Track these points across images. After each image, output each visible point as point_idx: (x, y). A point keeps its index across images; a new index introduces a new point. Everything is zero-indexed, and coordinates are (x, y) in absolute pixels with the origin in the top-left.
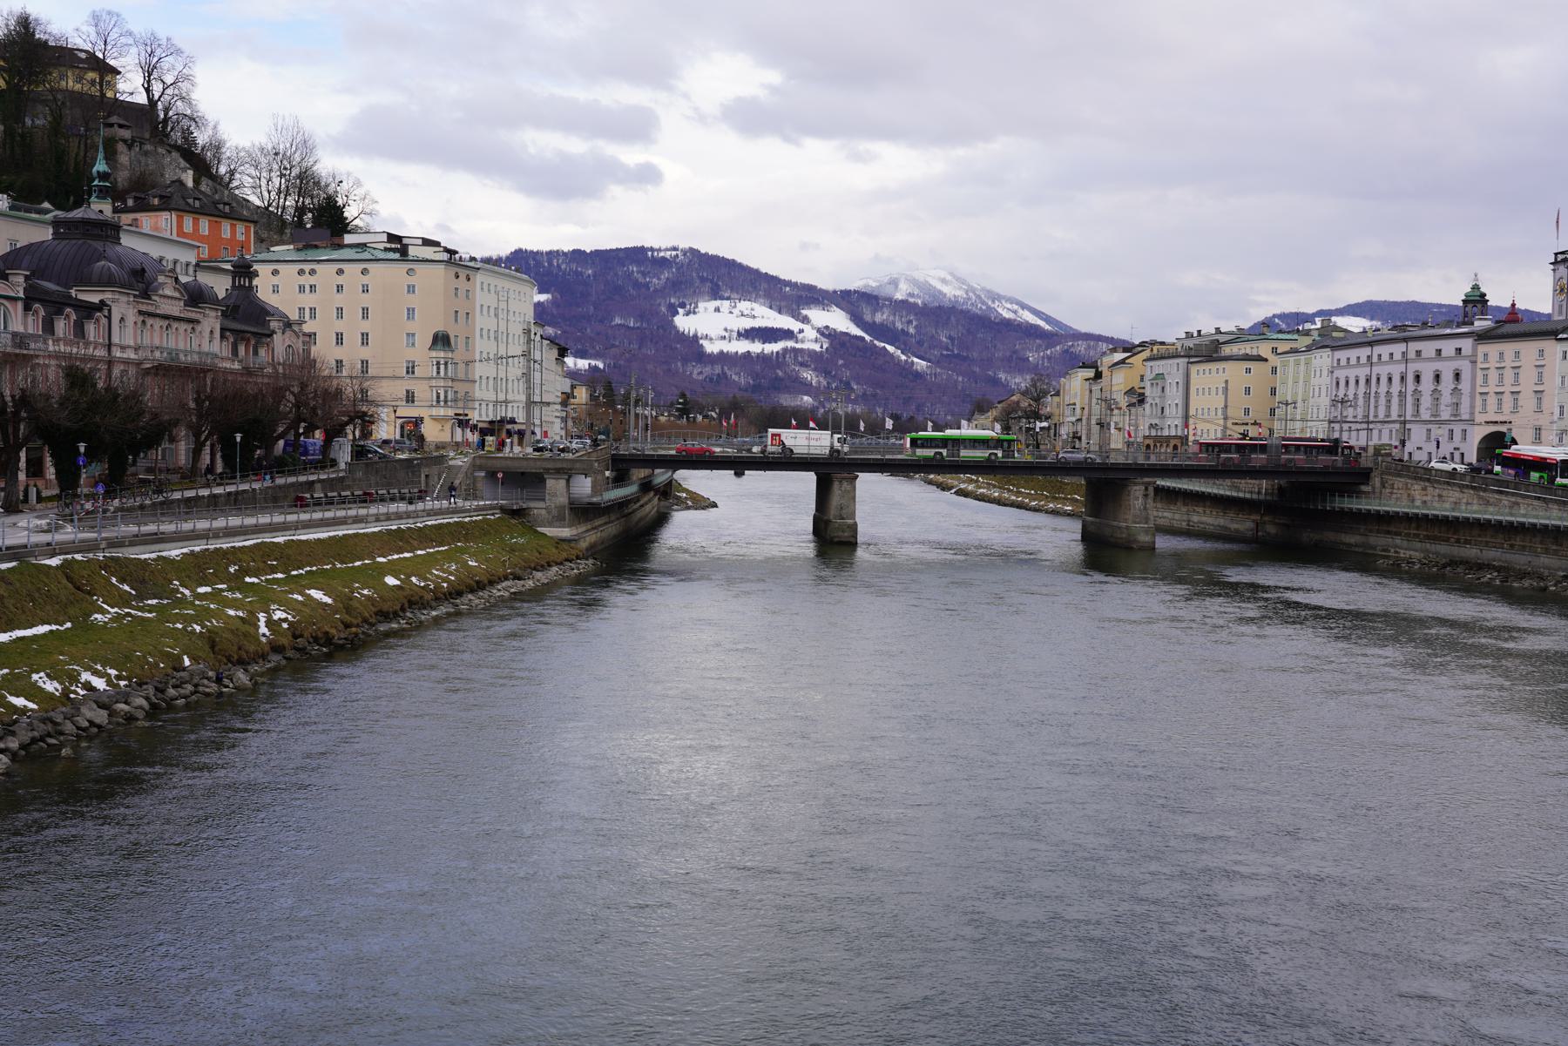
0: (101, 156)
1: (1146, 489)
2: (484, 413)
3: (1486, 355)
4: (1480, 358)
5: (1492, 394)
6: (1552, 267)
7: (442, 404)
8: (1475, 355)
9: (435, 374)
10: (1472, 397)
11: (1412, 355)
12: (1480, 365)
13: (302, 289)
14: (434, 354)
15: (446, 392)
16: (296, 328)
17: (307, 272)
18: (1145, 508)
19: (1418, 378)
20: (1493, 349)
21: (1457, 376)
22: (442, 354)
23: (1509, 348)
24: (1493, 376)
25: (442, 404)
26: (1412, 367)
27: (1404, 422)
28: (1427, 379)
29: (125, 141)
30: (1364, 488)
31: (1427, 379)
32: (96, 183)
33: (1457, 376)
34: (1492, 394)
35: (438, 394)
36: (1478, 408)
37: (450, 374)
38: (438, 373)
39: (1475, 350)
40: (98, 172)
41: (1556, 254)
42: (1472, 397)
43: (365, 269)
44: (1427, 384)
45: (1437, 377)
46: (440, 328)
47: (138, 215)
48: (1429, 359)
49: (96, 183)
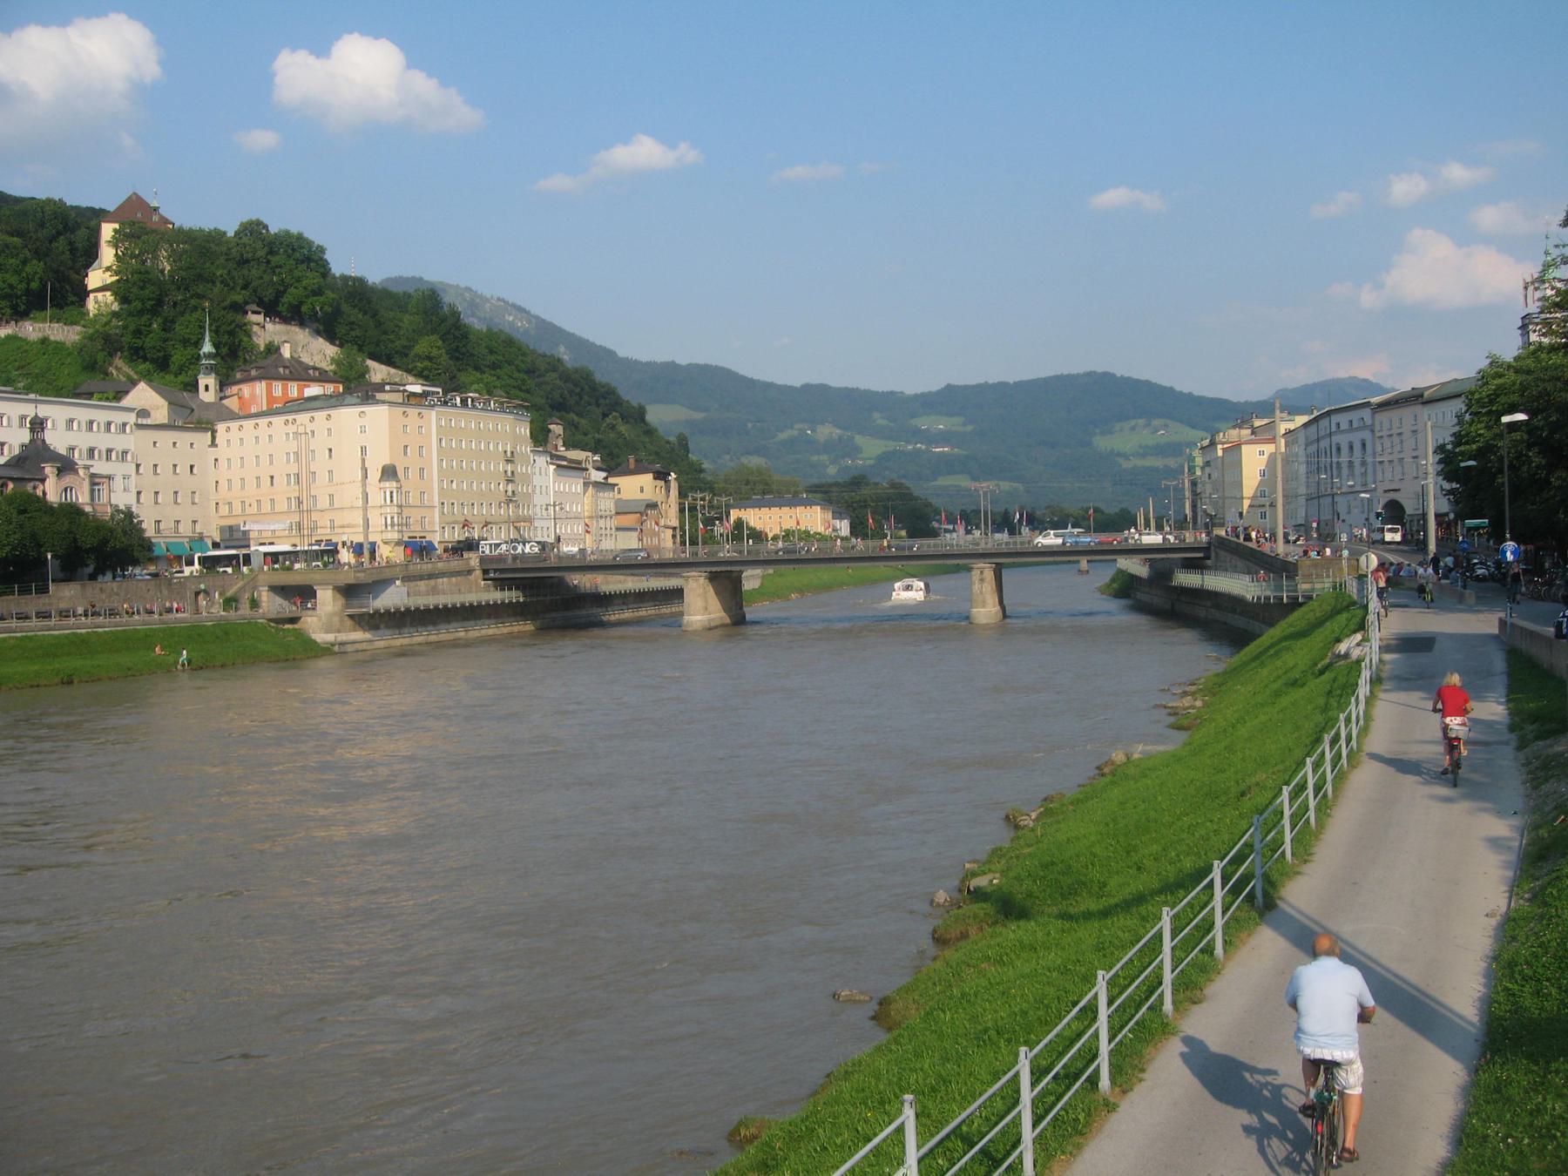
1: (982, 572)
3: (1381, 423)
4: (1377, 428)
6: (1520, 332)
7: (389, 528)
8: (1373, 425)
9: (383, 502)
11: (1334, 429)
12: (1378, 434)
13: (287, 434)
15: (392, 518)
16: (81, 472)
17: (290, 422)
19: (1339, 449)
20: (1383, 417)
21: (1364, 445)
22: (387, 484)
23: (1394, 414)
25: (389, 528)
26: (1335, 439)
27: (1333, 496)
28: (1345, 450)
29: (258, 324)
30: (1209, 562)
31: (1345, 450)
32: (204, 362)
33: (1364, 445)
35: (386, 518)
36: (1379, 477)
39: (1373, 417)
40: (204, 353)
41: (1522, 318)
43: (329, 415)
44: (1344, 459)
45: (1351, 448)
46: (387, 462)
47: (241, 386)
49: (204, 362)
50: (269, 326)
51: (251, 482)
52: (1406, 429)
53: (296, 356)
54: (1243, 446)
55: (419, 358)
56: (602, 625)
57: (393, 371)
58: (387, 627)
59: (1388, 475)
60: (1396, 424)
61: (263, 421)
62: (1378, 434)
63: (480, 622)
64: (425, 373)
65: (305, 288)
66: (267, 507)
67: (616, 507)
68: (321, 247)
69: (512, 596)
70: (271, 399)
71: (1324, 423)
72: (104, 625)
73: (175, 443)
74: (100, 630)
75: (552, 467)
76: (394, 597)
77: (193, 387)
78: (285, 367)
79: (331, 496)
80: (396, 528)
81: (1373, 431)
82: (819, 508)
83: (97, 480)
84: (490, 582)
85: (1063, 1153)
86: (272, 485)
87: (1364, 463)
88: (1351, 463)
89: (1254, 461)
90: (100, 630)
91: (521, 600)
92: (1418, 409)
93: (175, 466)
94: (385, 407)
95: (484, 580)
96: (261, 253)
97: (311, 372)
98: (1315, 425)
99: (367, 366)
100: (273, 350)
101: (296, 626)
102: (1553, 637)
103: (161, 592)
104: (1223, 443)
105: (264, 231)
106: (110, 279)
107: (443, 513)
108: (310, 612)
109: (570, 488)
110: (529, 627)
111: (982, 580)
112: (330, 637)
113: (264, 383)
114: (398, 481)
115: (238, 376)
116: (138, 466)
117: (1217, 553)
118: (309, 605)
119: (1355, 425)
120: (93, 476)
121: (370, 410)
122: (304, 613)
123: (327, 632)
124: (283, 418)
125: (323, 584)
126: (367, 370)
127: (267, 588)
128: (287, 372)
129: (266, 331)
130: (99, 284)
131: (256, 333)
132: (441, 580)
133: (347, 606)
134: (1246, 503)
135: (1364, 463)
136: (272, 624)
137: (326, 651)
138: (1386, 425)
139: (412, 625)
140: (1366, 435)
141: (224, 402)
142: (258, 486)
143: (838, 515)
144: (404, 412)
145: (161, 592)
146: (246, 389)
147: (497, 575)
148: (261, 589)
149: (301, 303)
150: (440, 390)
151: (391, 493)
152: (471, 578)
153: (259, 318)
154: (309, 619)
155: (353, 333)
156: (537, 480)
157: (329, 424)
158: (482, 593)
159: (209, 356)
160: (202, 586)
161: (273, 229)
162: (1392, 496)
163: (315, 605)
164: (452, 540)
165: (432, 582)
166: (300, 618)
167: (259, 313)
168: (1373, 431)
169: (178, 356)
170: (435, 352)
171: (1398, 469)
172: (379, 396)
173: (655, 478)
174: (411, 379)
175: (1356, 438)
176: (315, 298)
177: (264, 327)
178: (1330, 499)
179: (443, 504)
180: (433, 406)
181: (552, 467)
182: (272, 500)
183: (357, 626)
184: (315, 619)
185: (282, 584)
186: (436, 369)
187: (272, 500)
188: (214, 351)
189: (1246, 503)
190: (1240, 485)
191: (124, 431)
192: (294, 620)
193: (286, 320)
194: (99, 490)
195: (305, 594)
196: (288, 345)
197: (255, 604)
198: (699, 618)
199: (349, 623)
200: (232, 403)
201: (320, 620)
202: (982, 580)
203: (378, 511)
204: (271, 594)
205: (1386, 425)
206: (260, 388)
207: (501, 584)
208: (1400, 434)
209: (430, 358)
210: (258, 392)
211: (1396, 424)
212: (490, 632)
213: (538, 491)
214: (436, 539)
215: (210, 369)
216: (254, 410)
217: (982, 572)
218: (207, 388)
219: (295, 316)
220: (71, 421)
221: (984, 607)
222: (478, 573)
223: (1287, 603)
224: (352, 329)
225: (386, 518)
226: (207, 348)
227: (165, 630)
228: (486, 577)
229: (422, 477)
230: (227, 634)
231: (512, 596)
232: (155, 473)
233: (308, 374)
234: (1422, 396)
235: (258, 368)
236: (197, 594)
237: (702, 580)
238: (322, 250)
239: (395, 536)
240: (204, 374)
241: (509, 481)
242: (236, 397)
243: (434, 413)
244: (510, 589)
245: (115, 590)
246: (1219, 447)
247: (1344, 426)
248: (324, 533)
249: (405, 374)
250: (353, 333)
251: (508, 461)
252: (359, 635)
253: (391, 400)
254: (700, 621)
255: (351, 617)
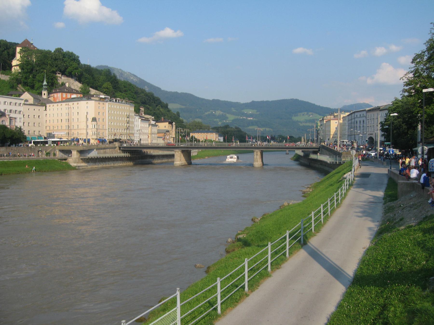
0: (45, 80)
1: (257, 153)
2: (110, 138)
5: (369, 126)
7: (94, 135)
8: (366, 116)
10: (366, 127)
11: (356, 117)
12: (367, 119)
13: (66, 108)
14: (92, 123)
15: (95, 132)
16: (7, 116)
18: (257, 158)
19: (357, 122)
20: (369, 114)
21: (364, 121)
24: (370, 121)
25: (94, 135)
26: (356, 119)
27: (355, 135)
28: (358, 122)
29: (60, 77)
31: (358, 122)
32: (44, 87)
33: (364, 121)
34: (369, 126)
36: (367, 130)
37: (96, 127)
38: (93, 127)
42: (366, 127)
44: (358, 125)
45: (360, 122)
46: (94, 116)
48: (359, 117)
50: (63, 78)
51: (56, 121)
52: (375, 117)
53: (70, 86)
54: (331, 121)
55: (104, 88)
56: (152, 163)
57: (97, 91)
58: (92, 162)
59: (370, 130)
60: (372, 116)
61: (59, 104)
62: (367, 119)
63: (118, 162)
64: (106, 92)
65: (73, 67)
66: (60, 128)
67: (158, 131)
68: (78, 56)
69: (127, 155)
70: (62, 98)
71: (353, 115)
72: (13, 160)
73: (34, 109)
74: (11, 160)
75: (140, 120)
76: (94, 154)
77: (41, 94)
78: (67, 89)
79: (78, 125)
80: (96, 135)
81: (366, 118)
82: (215, 134)
83: (12, 119)
84: (121, 151)
85: (231, 307)
86: (62, 122)
87: (363, 126)
88: (360, 126)
89: (334, 125)
90: (11, 160)
91: (130, 156)
92: (378, 112)
93: (34, 116)
94: (94, 101)
95: (119, 150)
96: (61, 57)
97: (74, 91)
98: (351, 116)
99: (90, 90)
100: (63, 84)
101: (66, 161)
102: (398, 174)
103: (28, 150)
104: (326, 120)
105: (62, 51)
106: (18, 63)
107: (109, 131)
108: (70, 157)
109: (145, 125)
110: (131, 164)
111: (257, 155)
112: (75, 165)
113: (60, 94)
114: (97, 122)
115: (53, 91)
116: (24, 115)
117: (322, 150)
118: (70, 156)
119: (361, 116)
120: (10, 118)
121: (89, 102)
122: (68, 158)
123: (75, 163)
124: (65, 103)
125: (73, 150)
126: (90, 91)
127: (58, 150)
128: (67, 91)
129: (62, 79)
130: (15, 64)
131: (59, 80)
132: (107, 150)
133: (80, 156)
134: (331, 136)
135: (363, 126)
136: (59, 160)
137: (74, 168)
138: (370, 116)
139: (99, 162)
140: (364, 119)
141: (50, 98)
142: (58, 122)
143: (220, 136)
144: (99, 103)
145: (28, 150)
146: (55, 95)
147: (123, 149)
148: (57, 150)
149: (72, 72)
150: (109, 97)
151: (95, 125)
152: (116, 149)
153: (60, 75)
154: (70, 159)
155: (86, 81)
156: (135, 123)
157: (78, 106)
158: (118, 154)
159: (45, 85)
160: (40, 149)
161: (65, 51)
162: (371, 136)
163: (71, 156)
164: (111, 139)
165: (105, 150)
166: (67, 159)
167: (60, 74)
168: (366, 118)
169: (37, 85)
170: (109, 87)
171: (373, 129)
172: (92, 98)
173: (169, 124)
174: (102, 94)
175: (361, 119)
176: (76, 70)
177: (61, 78)
178: (354, 136)
179: (109, 129)
180: (107, 101)
181: (140, 120)
182: (61, 126)
183: (83, 162)
184: (71, 159)
185: (62, 149)
186: (109, 91)
187: (61, 126)
188: (47, 84)
189: (331, 136)
190: (330, 131)
191: (20, 105)
192: (65, 160)
193: (67, 76)
194: (12, 122)
195: (68, 152)
196: (67, 83)
197: (55, 155)
198: (178, 163)
199: (81, 161)
200: (51, 99)
201: (73, 160)
202: (257, 155)
203: (91, 130)
204: (59, 152)
205: (370, 116)
206: (59, 95)
207: (124, 151)
208: (373, 119)
209: (107, 88)
210: (59, 96)
211: (372, 116)
212: (121, 165)
213: (136, 126)
214: (107, 138)
215: (46, 89)
216: (57, 101)
217: (257, 153)
218: (44, 94)
219: (70, 75)
220: (5, 102)
221: (257, 162)
222: (118, 148)
223: (338, 164)
224: (86, 79)
225: (93, 132)
226: (45, 83)
227: (29, 161)
228: (120, 149)
229: (103, 121)
230: (46, 163)
231: (127, 155)
232: (29, 117)
233: (73, 91)
234: (380, 108)
235: (59, 89)
236: (39, 151)
237: (180, 152)
238: (78, 57)
239: (95, 137)
240: (44, 90)
241: (128, 123)
242: (53, 97)
243: (107, 104)
244: (126, 153)
245: (15, 149)
246: (325, 120)
247: (358, 116)
248: (76, 136)
249: (100, 92)
250: (86, 81)
251: (128, 118)
252: (83, 164)
253: (96, 100)
254: (179, 163)
255: (82, 159)
